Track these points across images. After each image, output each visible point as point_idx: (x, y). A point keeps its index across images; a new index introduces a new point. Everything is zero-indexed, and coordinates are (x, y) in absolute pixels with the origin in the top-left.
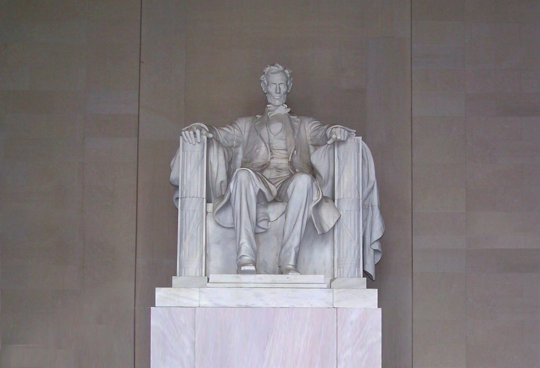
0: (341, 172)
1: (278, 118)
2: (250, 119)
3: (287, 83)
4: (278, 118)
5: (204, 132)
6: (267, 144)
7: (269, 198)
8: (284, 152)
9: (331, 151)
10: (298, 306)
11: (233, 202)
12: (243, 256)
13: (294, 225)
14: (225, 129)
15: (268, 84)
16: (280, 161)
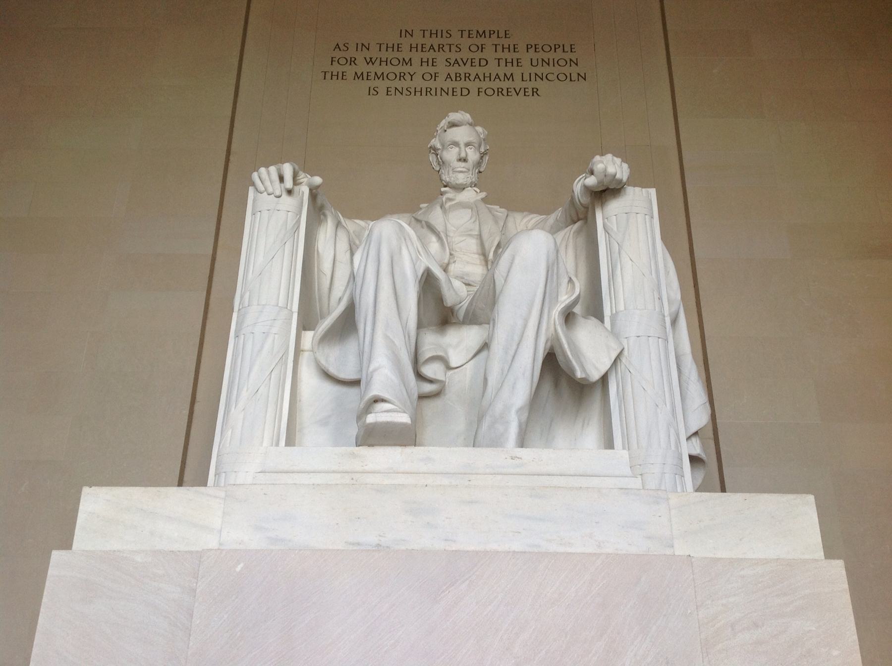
0: (616, 255)
1: (463, 205)
2: (408, 215)
3: (480, 146)
4: (463, 205)
5: (304, 178)
6: (442, 235)
7: (450, 299)
8: (477, 256)
9: (581, 240)
10: (553, 548)
11: (358, 291)
12: (377, 400)
13: (514, 357)
14: (357, 221)
15: (443, 145)
16: (469, 269)
